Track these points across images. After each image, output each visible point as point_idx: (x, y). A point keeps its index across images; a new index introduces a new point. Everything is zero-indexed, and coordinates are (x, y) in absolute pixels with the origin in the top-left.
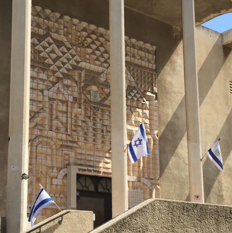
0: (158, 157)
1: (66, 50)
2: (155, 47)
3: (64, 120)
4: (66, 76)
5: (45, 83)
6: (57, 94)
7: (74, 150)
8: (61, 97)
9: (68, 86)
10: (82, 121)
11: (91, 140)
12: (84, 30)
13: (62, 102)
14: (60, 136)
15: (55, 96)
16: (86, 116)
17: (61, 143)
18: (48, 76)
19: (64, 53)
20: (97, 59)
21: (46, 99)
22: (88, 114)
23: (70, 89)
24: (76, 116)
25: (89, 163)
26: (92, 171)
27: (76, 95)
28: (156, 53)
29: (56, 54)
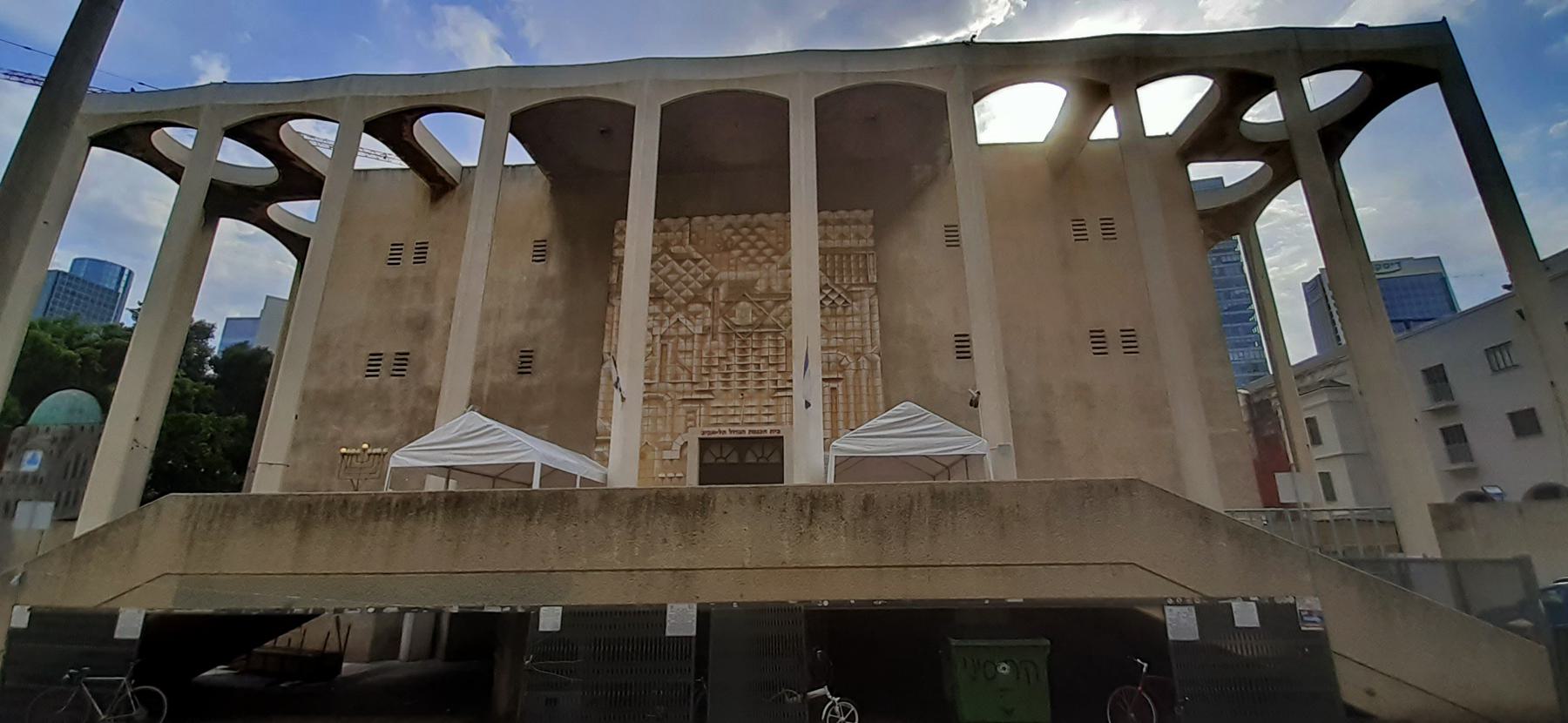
0: (880, 390)
1: (692, 264)
2: (871, 212)
3: (688, 362)
4: (695, 300)
5: (657, 318)
6: (677, 329)
8: (683, 330)
9: (695, 314)
10: (720, 358)
11: (735, 386)
12: (730, 226)
13: (685, 338)
14: (679, 387)
15: (672, 331)
17: (681, 398)
18: (663, 307)
19: (687, 269)
20: (752, 261)
21: (658, 338)
23: (699, 316)
24: (710, 353)
26: (728, 432)
27: (708, 322)
28: (873, 221)
29: (677, 273)
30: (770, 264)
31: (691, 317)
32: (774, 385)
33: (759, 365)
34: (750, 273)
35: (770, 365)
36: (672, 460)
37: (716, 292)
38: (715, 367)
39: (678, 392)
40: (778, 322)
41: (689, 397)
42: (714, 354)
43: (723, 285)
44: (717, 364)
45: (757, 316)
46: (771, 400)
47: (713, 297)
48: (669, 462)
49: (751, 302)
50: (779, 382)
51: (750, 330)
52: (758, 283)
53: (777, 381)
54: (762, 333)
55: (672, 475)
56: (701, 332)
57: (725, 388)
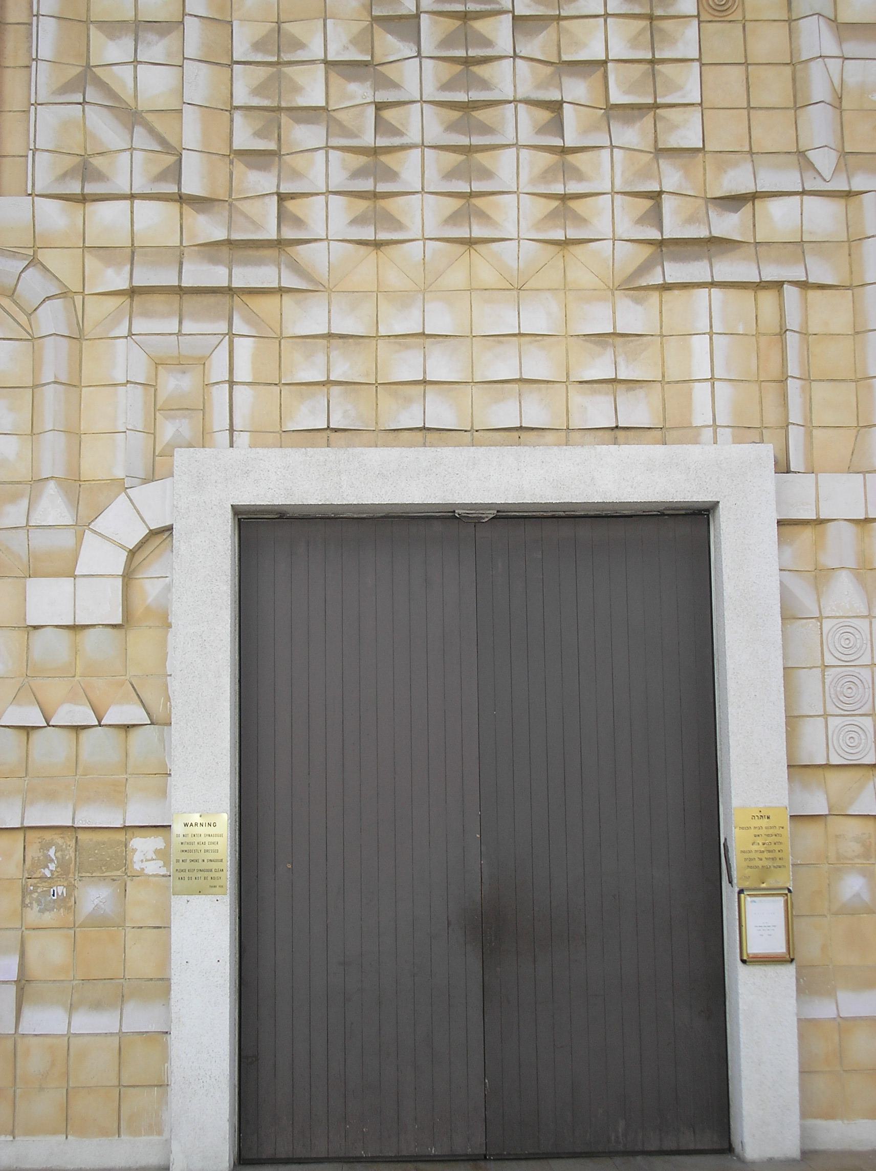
7: (253, 319)
25: (416, 409)
32: (641, 221)
33: (556, 107)
35: (613, 112)
36: (74, 628)
38: (309, 114)
39: (106, 252)
41: (168, 278)
42: (299, 45)
44: (319, 100)
46: (625, 304)
48: (61, 643)
50: (668, 204)
53: (656, 196)
55: (84, 715)
57: (368, 233)
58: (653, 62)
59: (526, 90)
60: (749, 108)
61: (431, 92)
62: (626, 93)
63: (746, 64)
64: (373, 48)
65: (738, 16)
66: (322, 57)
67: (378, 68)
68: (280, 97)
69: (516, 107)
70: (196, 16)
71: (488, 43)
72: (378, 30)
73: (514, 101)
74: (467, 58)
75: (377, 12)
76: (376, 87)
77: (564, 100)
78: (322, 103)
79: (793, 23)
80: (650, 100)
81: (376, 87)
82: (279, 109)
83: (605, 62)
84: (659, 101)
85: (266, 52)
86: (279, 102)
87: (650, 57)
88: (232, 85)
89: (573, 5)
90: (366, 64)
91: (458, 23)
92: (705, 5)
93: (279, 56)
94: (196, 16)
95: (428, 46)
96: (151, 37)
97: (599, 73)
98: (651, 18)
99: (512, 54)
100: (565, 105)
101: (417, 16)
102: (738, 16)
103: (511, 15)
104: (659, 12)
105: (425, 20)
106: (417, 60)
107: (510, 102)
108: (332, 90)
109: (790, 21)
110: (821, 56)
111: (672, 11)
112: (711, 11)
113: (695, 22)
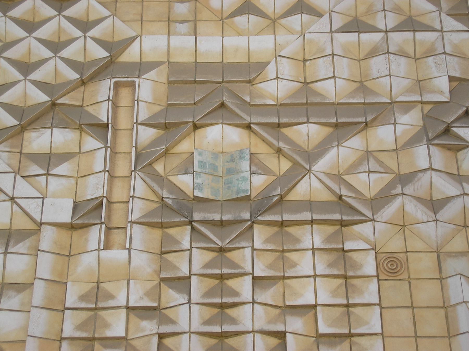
16: (163, 280)
22: (176, 268)
23: (62, 169)
30: (306, 17)
31: (35, 169)
33: (281, 335)
34: (242, 41)
37: (125, 93)
40: (344, 192)
42: (111, 297)
43: (152, 74)
45: (266, 171)
47: (115, 106)
49: (248, 127)
51: (247, 216)
52: (271, 71)
54: (282, 224)
56: (66, 217)
58: (347, 306)
59: (260, 324)
60: (416, 337)
61: (196, 326)
62: (330, 326)
63: (413, 307)
64: (160, 298)
65: (405, 276)
66: (125, 303)
67: (163, 311)
68: (94, 331)
69: (254, 336)
70: (42, 279)
71: (236, 294)
72: (164, 287)
73: (253, 331)
74: (222, 303)
75: (163, 275)
76: (160, 324)
77: (287, 330)
78: (123, 334)
79: (443, 281)
80: (346, 331)
81: (160, 324)
82: (93, 339)
83: (315, 306)
84: (353, 331)
85: (88, 301)
86: (94, 334)
87: (345, 302)
88: (63, 323)
89: (293, 270)
90: (154, 309)
91: (217, 282)
92: (382, 269)
93: (96, 304)
94: (42, 279)
95: (195, 297)
96: (11, 293)
97: (312, 313)
98: (345, 277)
99: (251, 301)
100: (287, 334)
101: (190, 278)
102: (405, 276)
103: (251, 276)
104: (350, 274)
105: (194, 280)
106: (188, 305)
107: (250, 332)
108: (131, 326)
109: (441, 279)
110: (464, 302)
111: (359, 273)
112: (386, 273)
113: (376, 280)
